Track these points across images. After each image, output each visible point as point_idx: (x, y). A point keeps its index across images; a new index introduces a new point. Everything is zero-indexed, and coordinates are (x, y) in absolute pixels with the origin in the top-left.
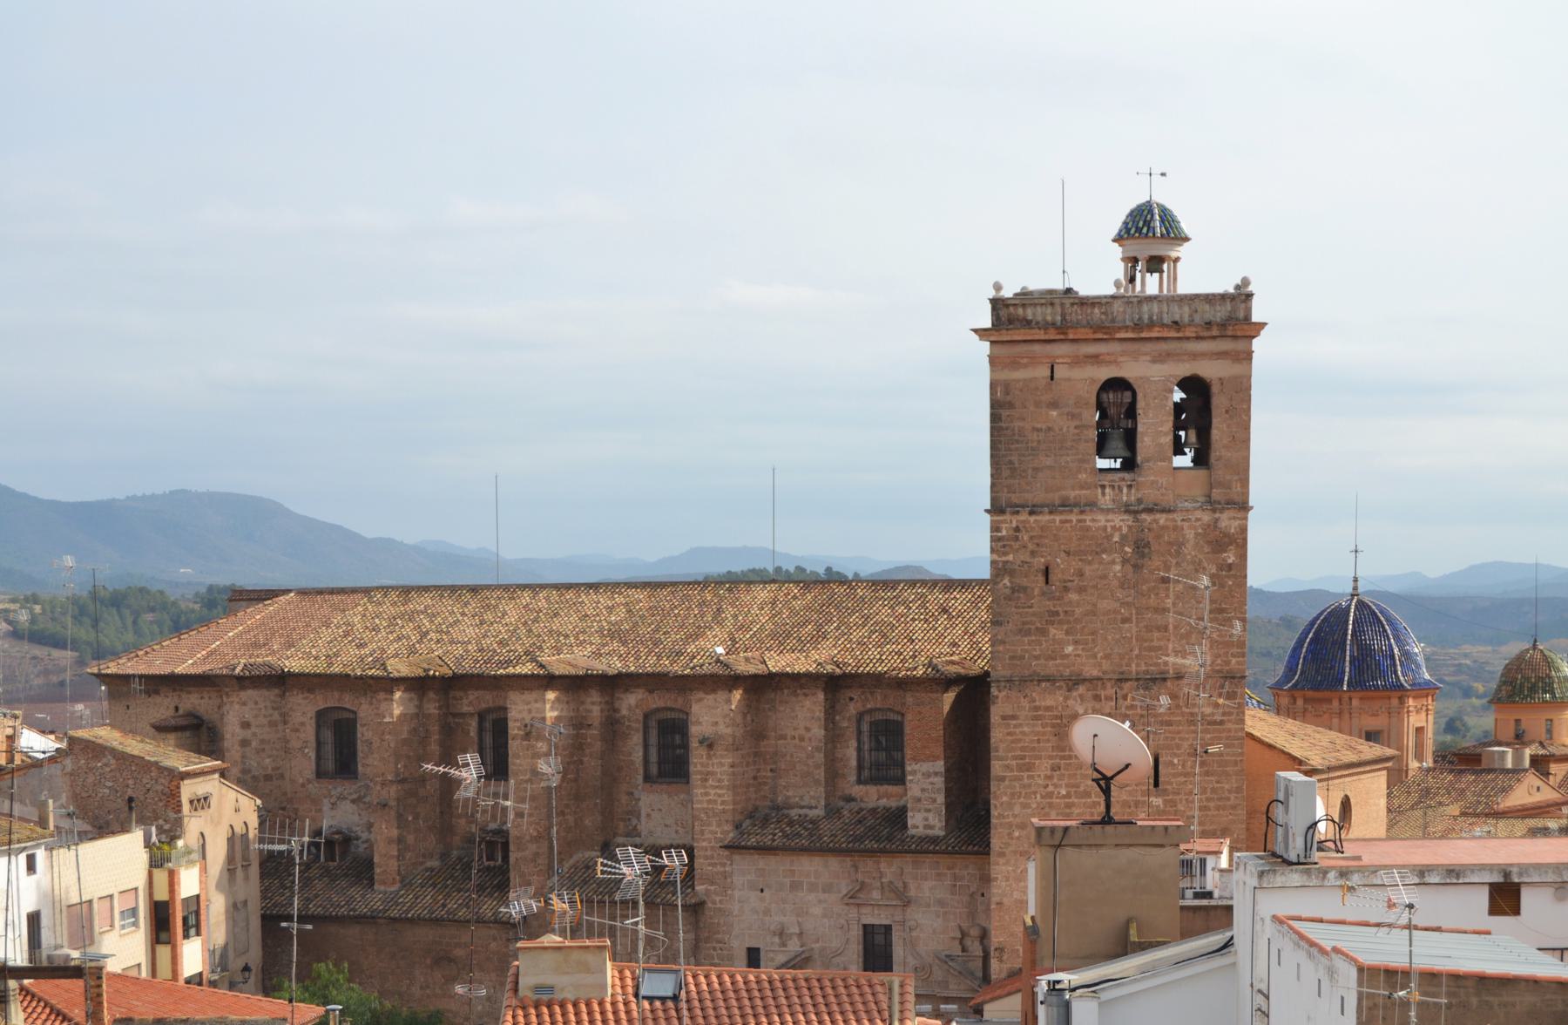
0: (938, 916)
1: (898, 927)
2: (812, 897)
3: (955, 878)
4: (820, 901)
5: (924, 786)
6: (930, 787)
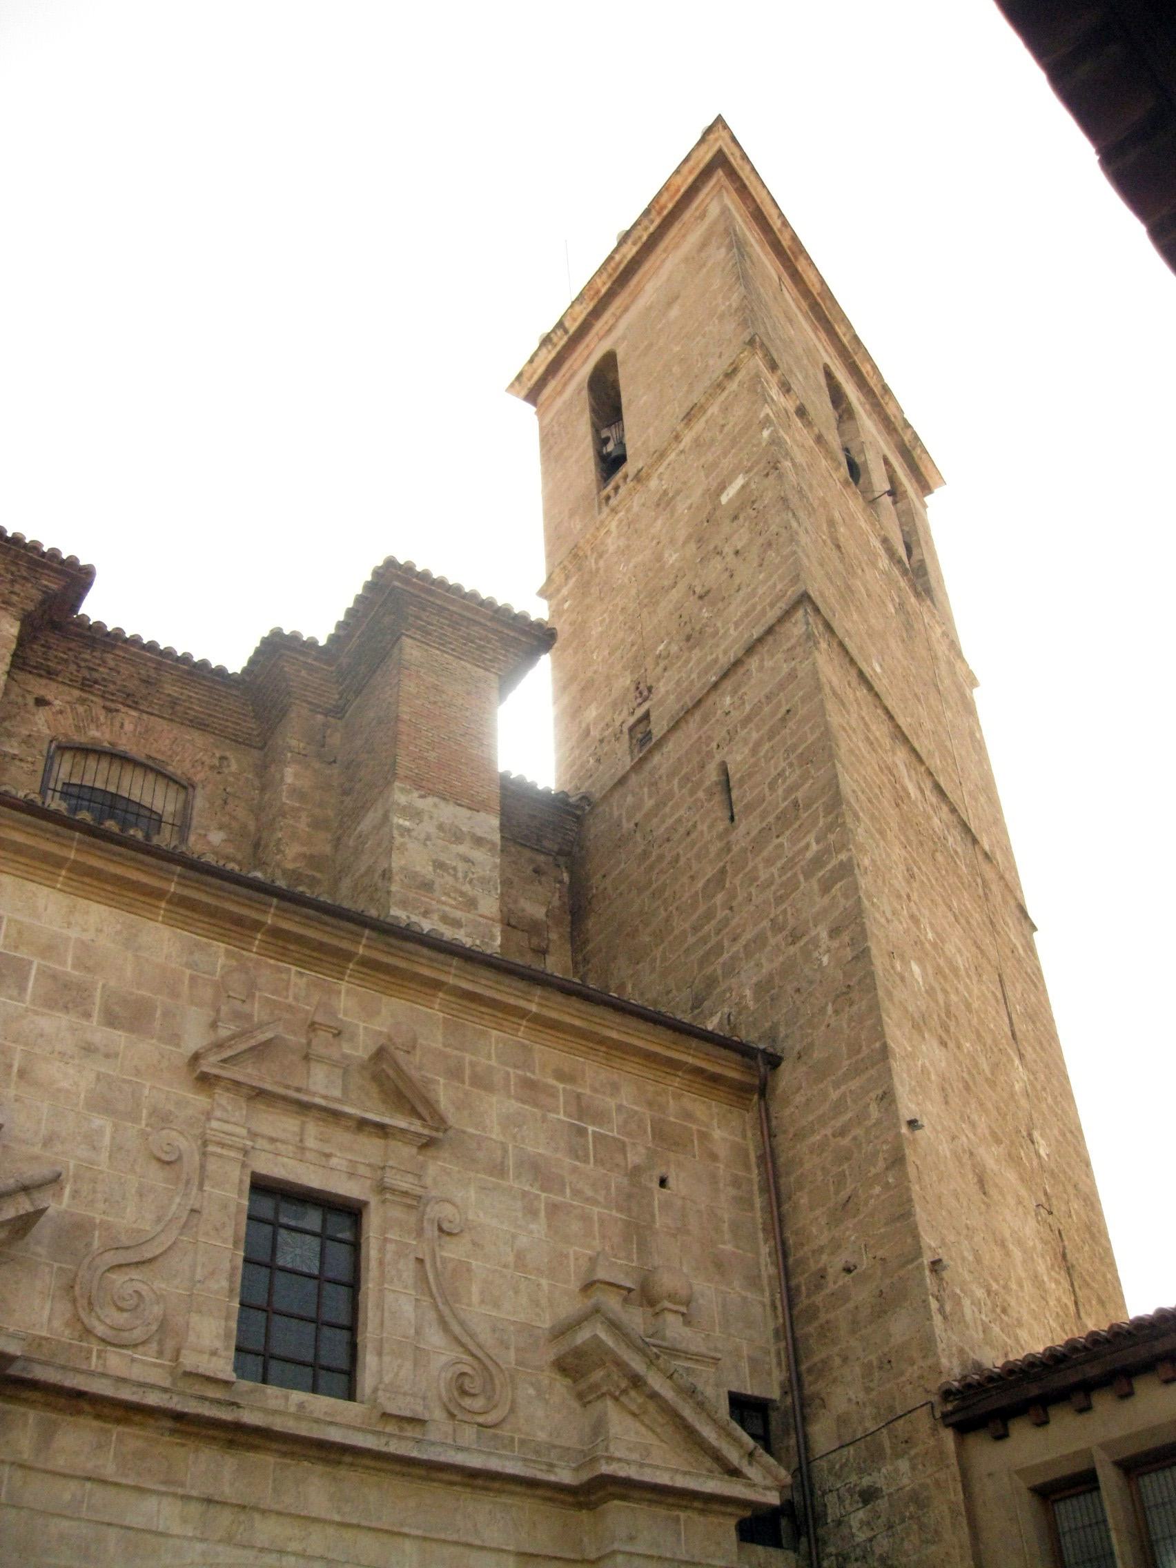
0: (532, 1213)
1: (396, 1213)
2: (54, 1024)
3: (582, 1109)
4: (89, 1049)
5: (443, 857)
6: (461, 867)
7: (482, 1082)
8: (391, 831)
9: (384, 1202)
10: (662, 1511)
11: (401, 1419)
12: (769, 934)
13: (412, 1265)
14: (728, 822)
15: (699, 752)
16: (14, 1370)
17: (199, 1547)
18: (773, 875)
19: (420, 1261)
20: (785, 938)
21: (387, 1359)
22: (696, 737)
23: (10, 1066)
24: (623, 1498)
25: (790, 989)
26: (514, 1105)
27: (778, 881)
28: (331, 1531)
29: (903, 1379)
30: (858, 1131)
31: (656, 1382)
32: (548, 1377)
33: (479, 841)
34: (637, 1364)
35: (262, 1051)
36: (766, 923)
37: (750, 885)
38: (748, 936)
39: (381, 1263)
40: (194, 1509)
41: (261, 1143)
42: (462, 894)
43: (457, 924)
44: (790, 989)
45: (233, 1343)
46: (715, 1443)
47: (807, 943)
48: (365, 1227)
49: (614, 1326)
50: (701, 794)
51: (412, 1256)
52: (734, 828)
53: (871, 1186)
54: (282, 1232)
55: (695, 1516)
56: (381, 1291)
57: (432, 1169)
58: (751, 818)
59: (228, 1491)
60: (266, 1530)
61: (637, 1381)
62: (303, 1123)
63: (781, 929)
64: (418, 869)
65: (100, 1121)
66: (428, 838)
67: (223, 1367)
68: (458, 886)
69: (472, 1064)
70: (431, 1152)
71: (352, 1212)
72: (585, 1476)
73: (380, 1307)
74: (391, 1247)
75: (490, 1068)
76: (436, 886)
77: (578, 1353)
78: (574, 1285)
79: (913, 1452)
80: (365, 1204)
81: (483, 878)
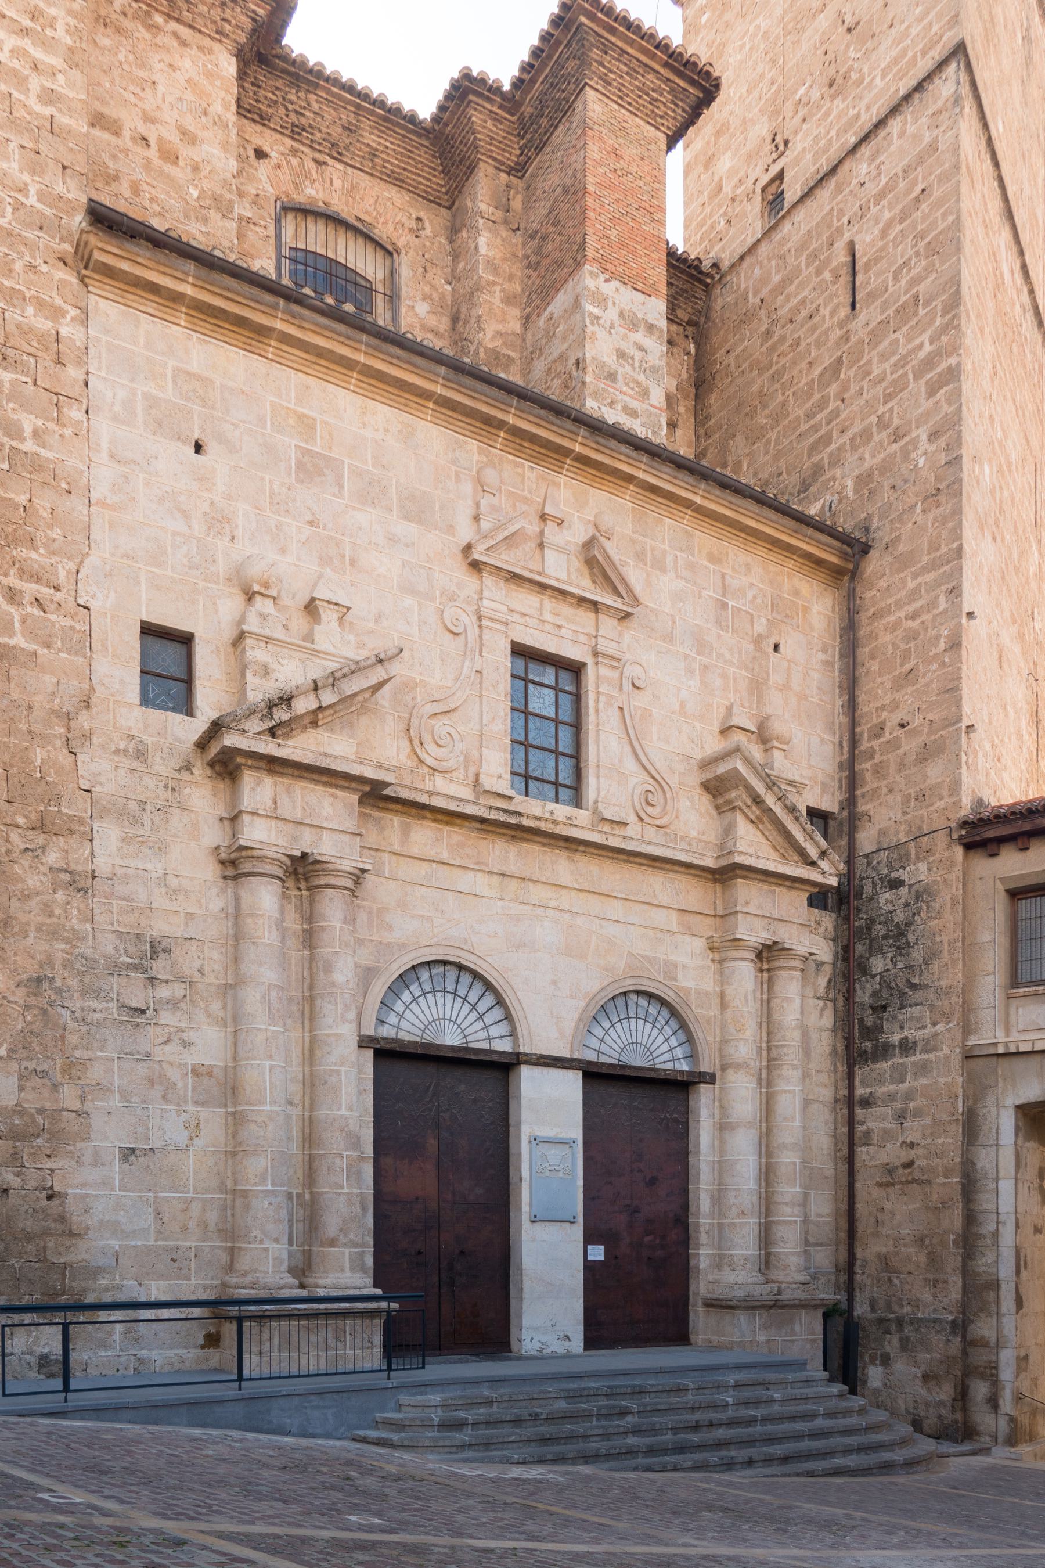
5: (626, 347)
6: (638, 355)
7: (660, 565)
8: (584, 321)
9: (597, 663)
10: (765, 887)
11: (613, 822)
12: (874, 429)
13: (617, 712)
14: (849, 308)
15: (829, 227)
16: (387, 792)
17: (499, 903)
18: (884, 372)
19: (621, 709)
20: (888, 436)
21: (602, 780)
22: (829, 208)
23: (344, 556)
24: (744, 877)
25: (886, 486)
26: (680, 584)
27: (889, 378)
28: (573, 893)
29: (933, 808)
30: (925, 617)
31: (770, 801)
32: (698, 791)
33: (651, 328)
34: (760, 788)
35: (511, 541)
36: (874, 419)
37: (863, 379)
38: (856, 429)
39: (597, 711)
40: (495, 879)
41: (516, 618)
42: (638, 383)
43: (633, 414)
44: (886, 486)
45: (509, 770)
46: (803, 844)
47: (907, 444)
48: (583, 683)
49: (748, 761)
50: (827, 275)
51: (616, 705)
52: (855, 317)
53: (930, 663)
54: (531, 686)
55: (784, 890)
56: (598, 731)
57: (627, 638)
58: (872, 309)
59: (513, 869)
60: (538, 893)
61: (758, 800)
62: (542, 600)
63: (887, 426)
64: (605, 359)
65: (409, 601)
66: (612, 327)
67: (504, 786)
68: (636, 376)
69: (653, 549)
70: (625, 623)
71: (576, 669)
72: (723, 862)
73: (597, 742)
74: (602, 698)
75: (665, 551)
76: (619, 377)
77: (719, 778)
78: (716, 727)
79: (931, 859)
80: (584, 665)
81: (653, 367)
